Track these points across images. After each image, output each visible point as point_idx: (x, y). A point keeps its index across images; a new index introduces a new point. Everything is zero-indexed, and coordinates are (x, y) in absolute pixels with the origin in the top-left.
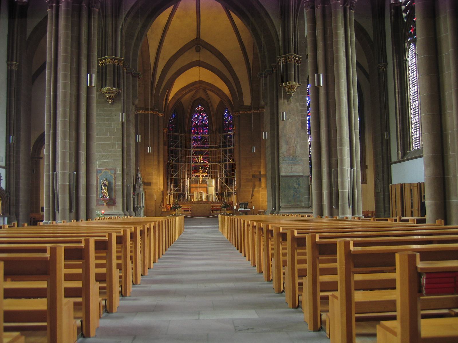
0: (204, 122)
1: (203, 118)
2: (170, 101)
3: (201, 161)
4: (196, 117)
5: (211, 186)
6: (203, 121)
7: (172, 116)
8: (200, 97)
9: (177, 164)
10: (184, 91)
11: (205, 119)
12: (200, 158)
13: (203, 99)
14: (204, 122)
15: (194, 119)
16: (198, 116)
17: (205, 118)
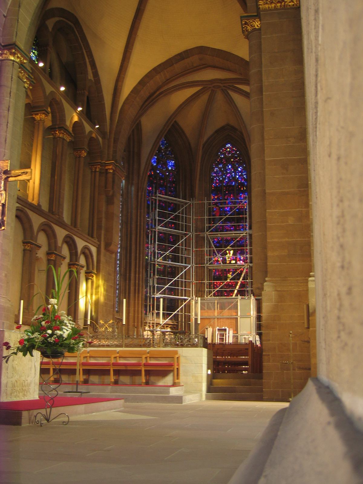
0: (237, 177)
1: (236, 170)
2: (127, 99)
3: (230, 261)
4: (220, 168)
5: (246, 316)
6: (236, 175)
7: (165, 164)
8: (228, 125)
9: (175, 267)
10: (160, 72)
11: (240, 172)
12: (230, 253)
13: (233, 129)
14: (237, 177)
15: (215, 173)
16: (224, 167)
17: (239, 169)
